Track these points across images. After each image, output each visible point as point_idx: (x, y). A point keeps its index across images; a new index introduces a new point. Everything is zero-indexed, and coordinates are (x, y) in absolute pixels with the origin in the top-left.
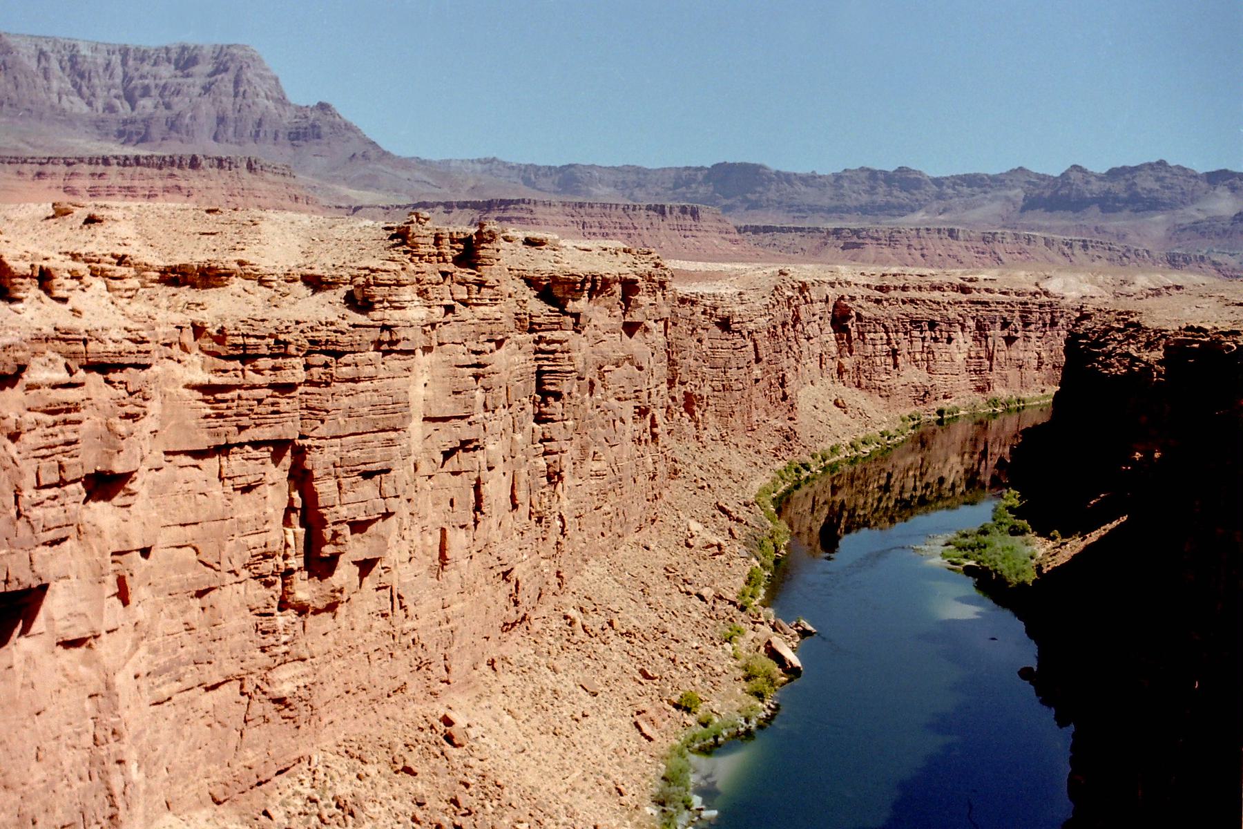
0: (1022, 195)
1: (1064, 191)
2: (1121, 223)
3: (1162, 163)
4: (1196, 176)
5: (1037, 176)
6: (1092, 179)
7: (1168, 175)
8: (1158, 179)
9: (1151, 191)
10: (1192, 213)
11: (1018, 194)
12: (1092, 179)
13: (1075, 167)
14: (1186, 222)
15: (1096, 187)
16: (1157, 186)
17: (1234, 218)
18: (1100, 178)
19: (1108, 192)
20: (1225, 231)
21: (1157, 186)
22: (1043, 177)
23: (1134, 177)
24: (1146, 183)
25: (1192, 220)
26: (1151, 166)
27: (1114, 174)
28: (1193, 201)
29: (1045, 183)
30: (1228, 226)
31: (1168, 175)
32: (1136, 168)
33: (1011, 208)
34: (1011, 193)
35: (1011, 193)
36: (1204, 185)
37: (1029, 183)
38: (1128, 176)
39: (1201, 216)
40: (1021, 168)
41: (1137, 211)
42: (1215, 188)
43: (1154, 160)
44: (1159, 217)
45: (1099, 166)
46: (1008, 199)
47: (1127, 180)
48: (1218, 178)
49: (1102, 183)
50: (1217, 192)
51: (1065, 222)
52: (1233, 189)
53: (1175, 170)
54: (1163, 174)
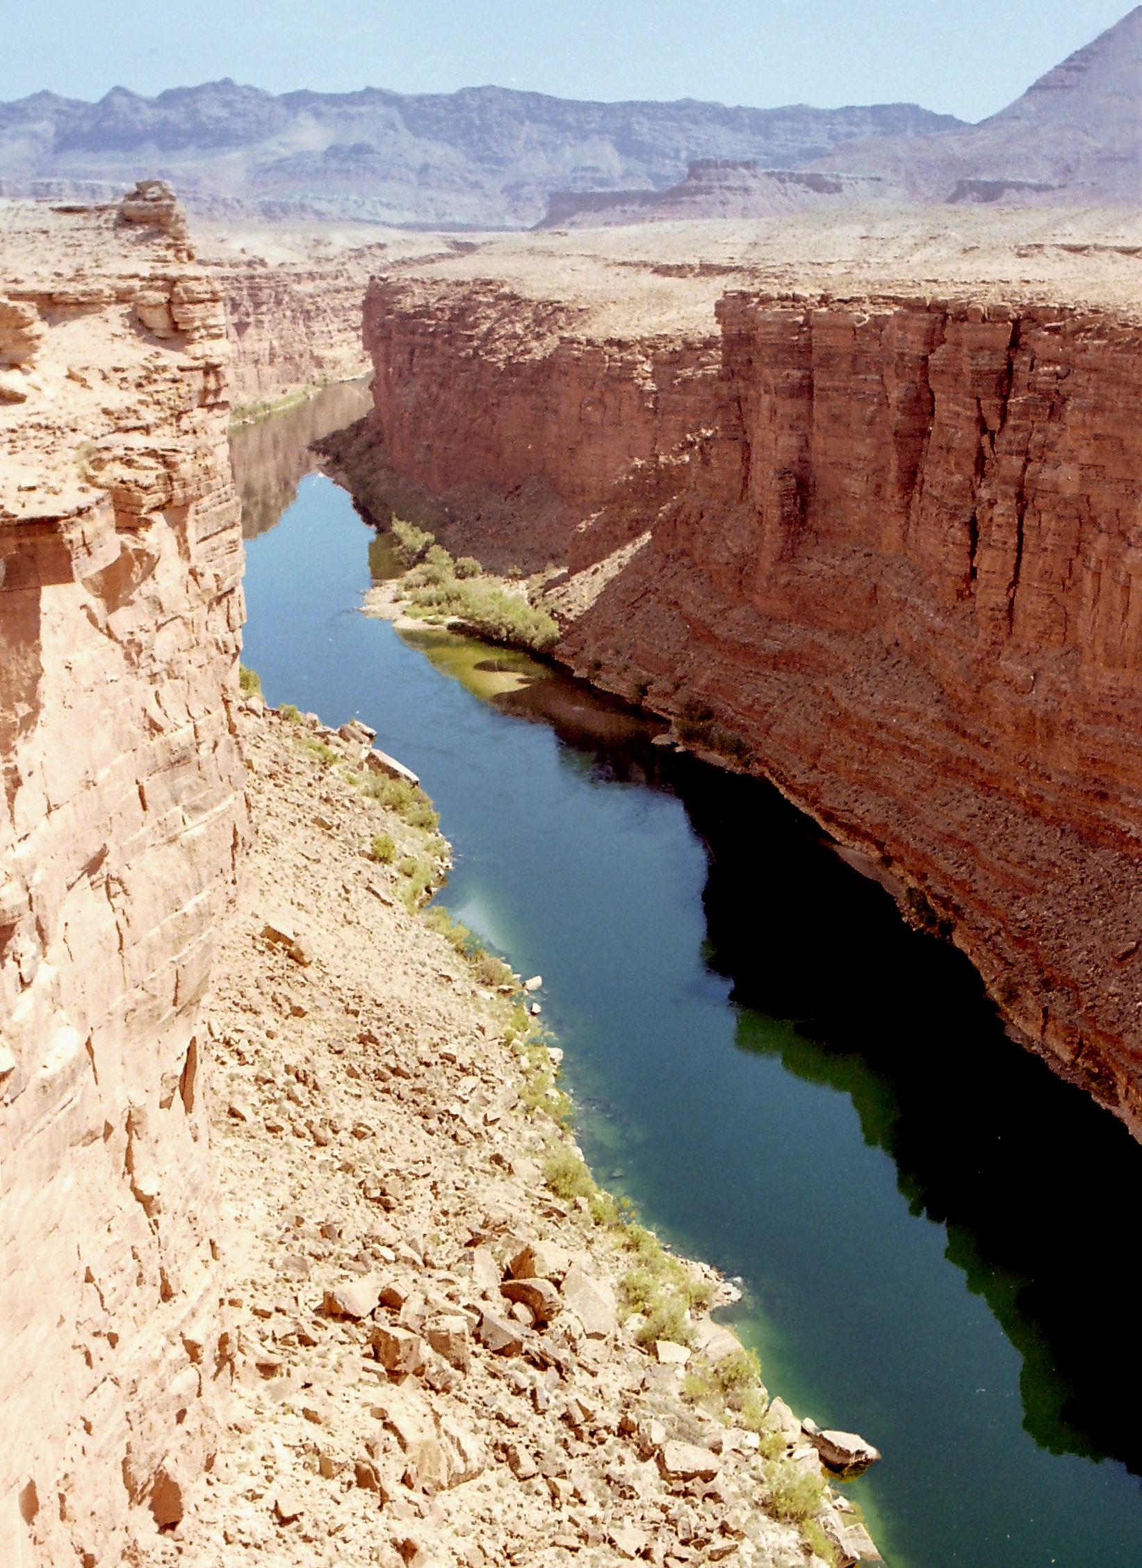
0: (52, 130)
1: (108, 123)
2: (189, 165)
3: (227, 83)
4: (269, 99)
5: (69, 102)
6: (143, 106)
7: (238, 98)
8: (227, 104)
9: (219, 120)
10: (273, 148)
11: (45, 127)
12: (143, 106)
13: (118, 90)
14: (270, 160)
15: (148, 115)
16: (224, 113)
17: (326, 154)
18: (153, 104)
19: (165, 122)
20: (317, 171)
21: (224, 113)
22: (76, 105)
23: (195, 102)
24: (212, 110)
25: (276, 158)
26: (215, 86)
27: (169, 98)
28: (272, 131)
29: (80, 112)
30: (320, 164)
31: (238, 98)
32: (198, 90)
33: (41, 149)
34: (39, 127)
35: (39, 127)
36: (281, 111)
37: (59, 112)
38: (187, 100)
39: (286, 153)
40: (45, 94)
41: (204, 147)
42: (295, 115)
43: (218, 78)
44: (234, 155)
45: (149, 89)
46: (35, 136)
47: (187, 106)
48: (298, 101)
49: (156, 111)
50: (299, 119)
51: (117, 166)
52: (318, 115)
53: (246, 92)
54: (230, 97)
